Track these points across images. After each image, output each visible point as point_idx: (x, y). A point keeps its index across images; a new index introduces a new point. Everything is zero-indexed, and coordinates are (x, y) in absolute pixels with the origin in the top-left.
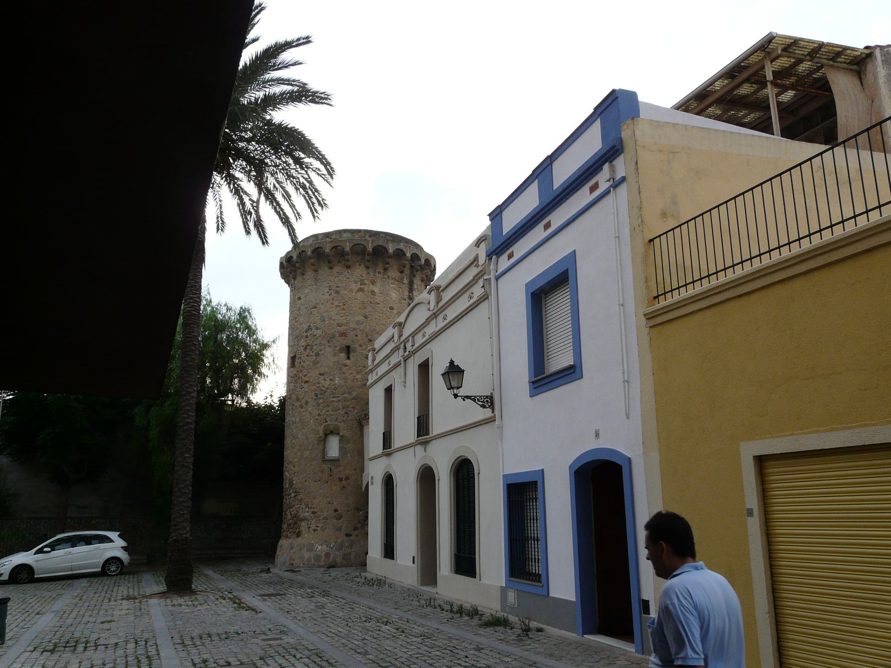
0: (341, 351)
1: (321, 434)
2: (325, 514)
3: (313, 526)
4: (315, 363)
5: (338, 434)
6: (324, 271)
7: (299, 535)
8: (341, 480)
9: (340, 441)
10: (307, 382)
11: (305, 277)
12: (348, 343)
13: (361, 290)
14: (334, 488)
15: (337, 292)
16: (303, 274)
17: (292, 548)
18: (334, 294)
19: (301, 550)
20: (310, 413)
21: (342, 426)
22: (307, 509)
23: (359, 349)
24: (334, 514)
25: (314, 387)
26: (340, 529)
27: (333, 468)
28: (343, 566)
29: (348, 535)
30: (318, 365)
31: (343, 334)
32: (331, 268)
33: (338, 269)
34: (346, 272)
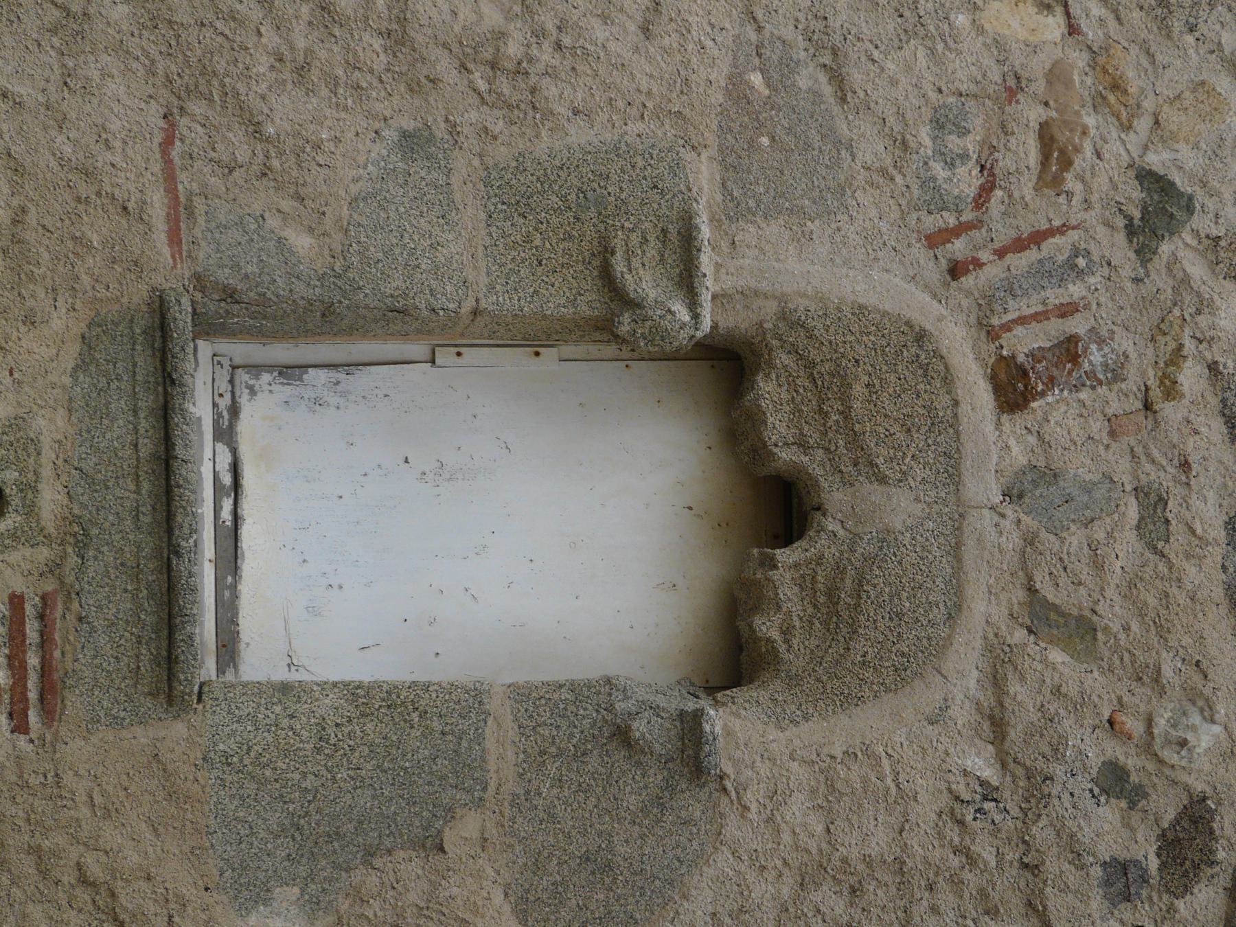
1: (757, 268)
5: (734, 657)
9: (588, 727)
21: (918, 738)
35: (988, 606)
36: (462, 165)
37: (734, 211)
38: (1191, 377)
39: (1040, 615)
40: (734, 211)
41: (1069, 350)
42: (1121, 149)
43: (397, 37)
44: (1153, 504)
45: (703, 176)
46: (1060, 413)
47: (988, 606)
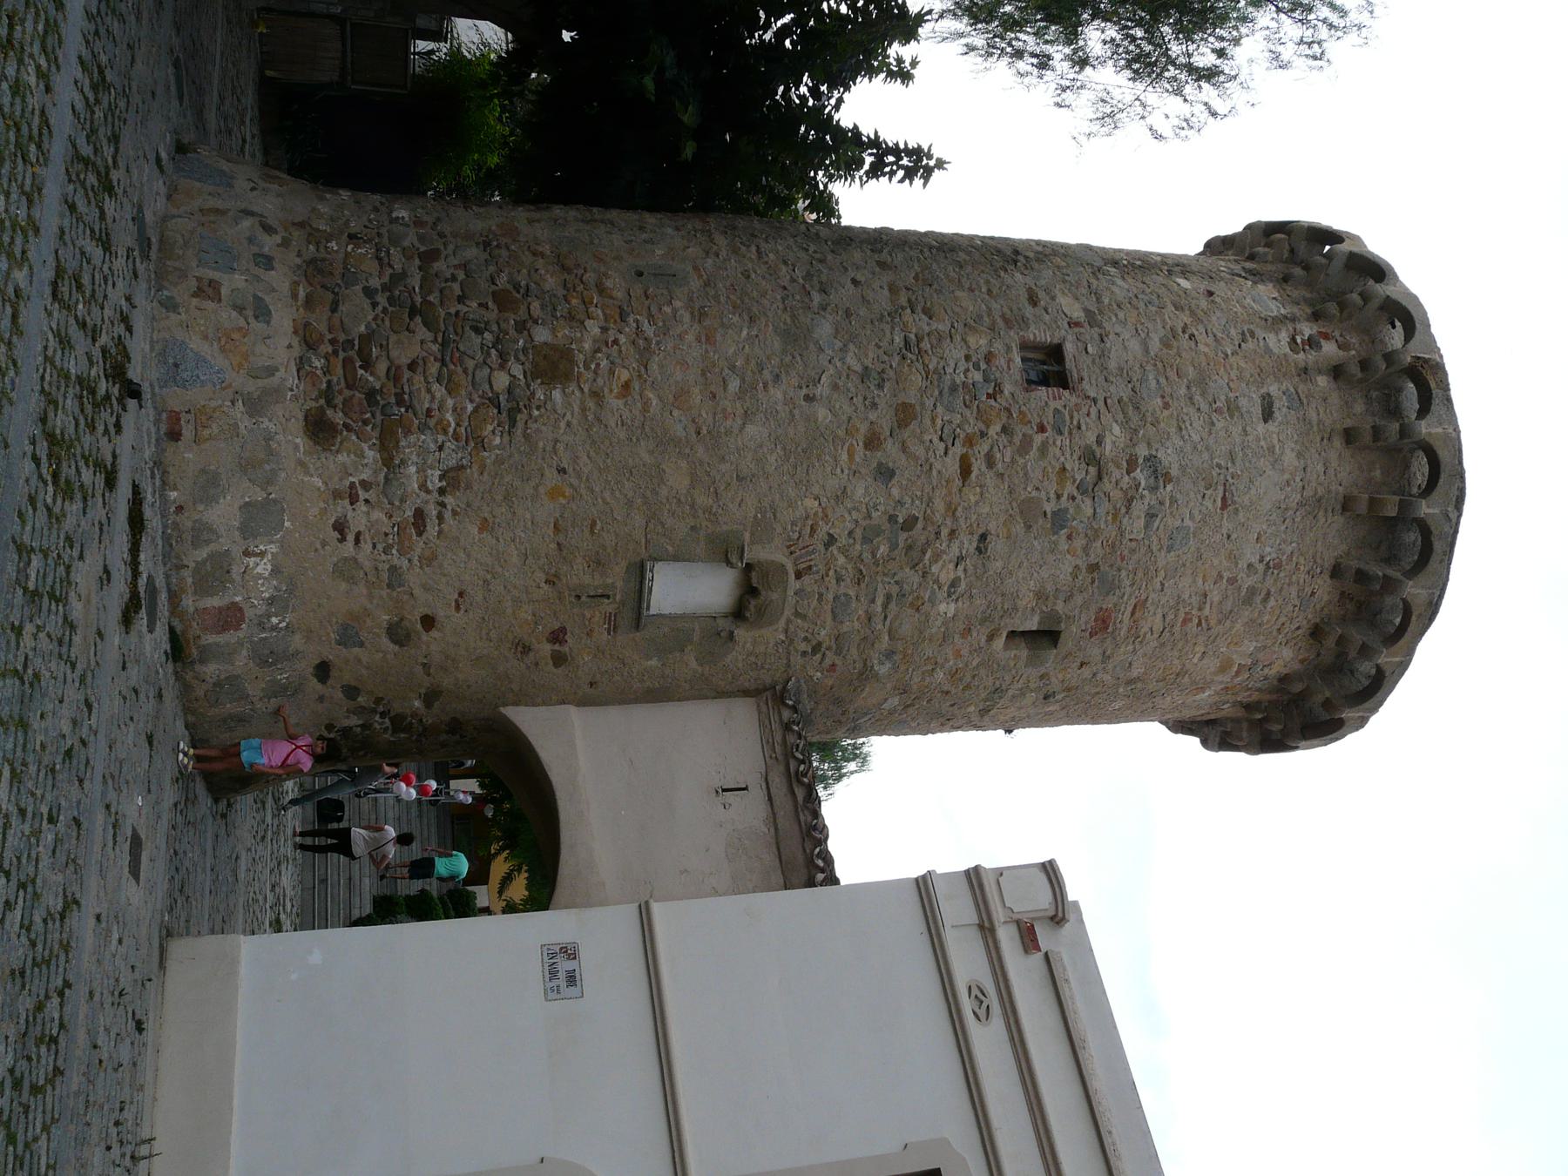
0: (1053, 616)
2: (414, 577)
3: (359, 518)
4: (1027, 511)
5: (738, 613)
6: (1331, 538)
7: (319, 429)
8: (557, 636)
10: (965, 471)
11: (1338, 442)
12: (1071, 635)
14: (526, 614)
16: (1349, 436)
17: (255, 406)
18: (1248, 582)
19: (246, 466)
20: (842, 495)
21: (773, 634)
22: (435, 482)
23: (1033, 673)
24: (414, 618)
25: (939, 505)
26: (348, 636)
27: (608, 607)
28: (185, 689)
29: (323, 670)
30: (1019, 528)
31: (1103, 623)
32: (1336, 572)
33: (1324, 589)
34: (1304, 620)
35: (788, 612)
36: (702, 533)
37: (752, 543)
38: (831, 573)
39: (797, 614)
40: (752, 543)
41: (810, 567)
42: (825, 528)
43: (692, 506)
44: (821, 595)
45: (747, 536)
46: (806, 579)
47: (788, 612)
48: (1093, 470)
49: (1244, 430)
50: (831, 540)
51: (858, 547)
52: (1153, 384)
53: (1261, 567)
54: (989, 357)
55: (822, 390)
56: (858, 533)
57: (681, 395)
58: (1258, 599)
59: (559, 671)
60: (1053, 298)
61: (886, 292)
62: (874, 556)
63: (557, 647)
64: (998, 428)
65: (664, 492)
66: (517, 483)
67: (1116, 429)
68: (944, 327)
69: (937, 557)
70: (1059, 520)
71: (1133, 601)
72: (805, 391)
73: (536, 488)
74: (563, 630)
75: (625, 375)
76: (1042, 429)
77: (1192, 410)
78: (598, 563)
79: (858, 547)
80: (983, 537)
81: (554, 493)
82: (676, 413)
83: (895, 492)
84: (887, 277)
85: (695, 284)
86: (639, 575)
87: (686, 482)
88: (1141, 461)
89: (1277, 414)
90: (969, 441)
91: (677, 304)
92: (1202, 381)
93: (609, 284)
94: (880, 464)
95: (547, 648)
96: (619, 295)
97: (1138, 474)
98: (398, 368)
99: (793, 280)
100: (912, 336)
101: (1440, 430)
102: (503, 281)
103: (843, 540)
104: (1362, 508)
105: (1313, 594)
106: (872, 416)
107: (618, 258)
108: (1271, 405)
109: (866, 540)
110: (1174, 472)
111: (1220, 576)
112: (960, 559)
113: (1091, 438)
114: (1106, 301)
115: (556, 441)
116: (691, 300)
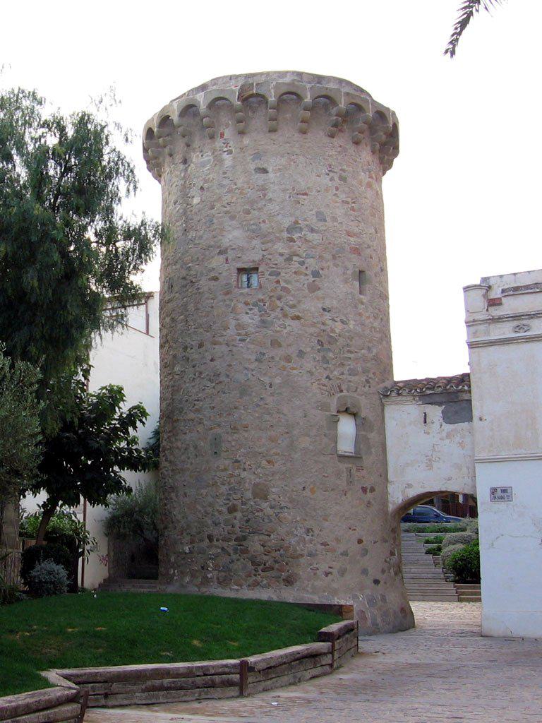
4: (313, 288)
5: (354, 415)
6: (318, 136)
8: (364, 490)
10: (298, 318)
13: (369, 185)
15: (342, 179)
18: (337, 182)
21: (363, 402)
25: (312, 330)
30: (319, 293)
31: (356, 251)
34: (351, 148)
35: (355, 395)
37: (330, 411)
40: (330, 411)
41: (338, 386)
45: (327, 413)
46: (343, 387)
47: (355, 395)
48: (295, 258)
49: (272, 183)
50: (328, 377)
51: (330, 366)
52: (254, 227)
53: (331, 174)
54: (246, 304)
55: (266, 380)
56: (325, 366)
57: (272, 439)
58: (344, 174)
59: (377, 490)
60: (214, 269)
61: (216, 347)
62: (333, 359)
63: (368, 491)
64: (278, 302)
65: (311, 448)
66: (309, 506)
67: (276, 247)
68: (233, 323)
69: (333, 331)
70: (316, 274)
71: (347, 237)
72: (268, 387)
73: (311, 499)
74: (362, 488)
75: (264, 462)
76: (278, 282)
77: (265, 209)
78: (338, 474)
79: (330, 366)
80: (324, 309)
81: (312, 491)
82: (279, 442)
83: (309, 349)
84: (208, 345)
85: (219, 431)
86: (343, 458)
87: (307, 438)
88: (290, 236)
89: (265, 166)
90: (285, 316)
91: (230, 439)
92: (252, 203)
93: (222, 467)
94: (298, 356)
95: (369, 494)
96: (227, 462)
97: (295, 236)
98: (265, 551)
99: (214, 388)
100: (238, 338)
101: (272, 91)
102: (224, 509)
103: (327, 373)
104: (304, 125)
105: (341, 146)
106: (277, 359)
107: (207, 462)
108: (259, 169)
109: (327, 362)
110: (293, 219)
111: (335, 195)
112: (333, 320)
113: (281, 259)
114: (212, 243)
115: (293, 491)
116: (228, 433)
